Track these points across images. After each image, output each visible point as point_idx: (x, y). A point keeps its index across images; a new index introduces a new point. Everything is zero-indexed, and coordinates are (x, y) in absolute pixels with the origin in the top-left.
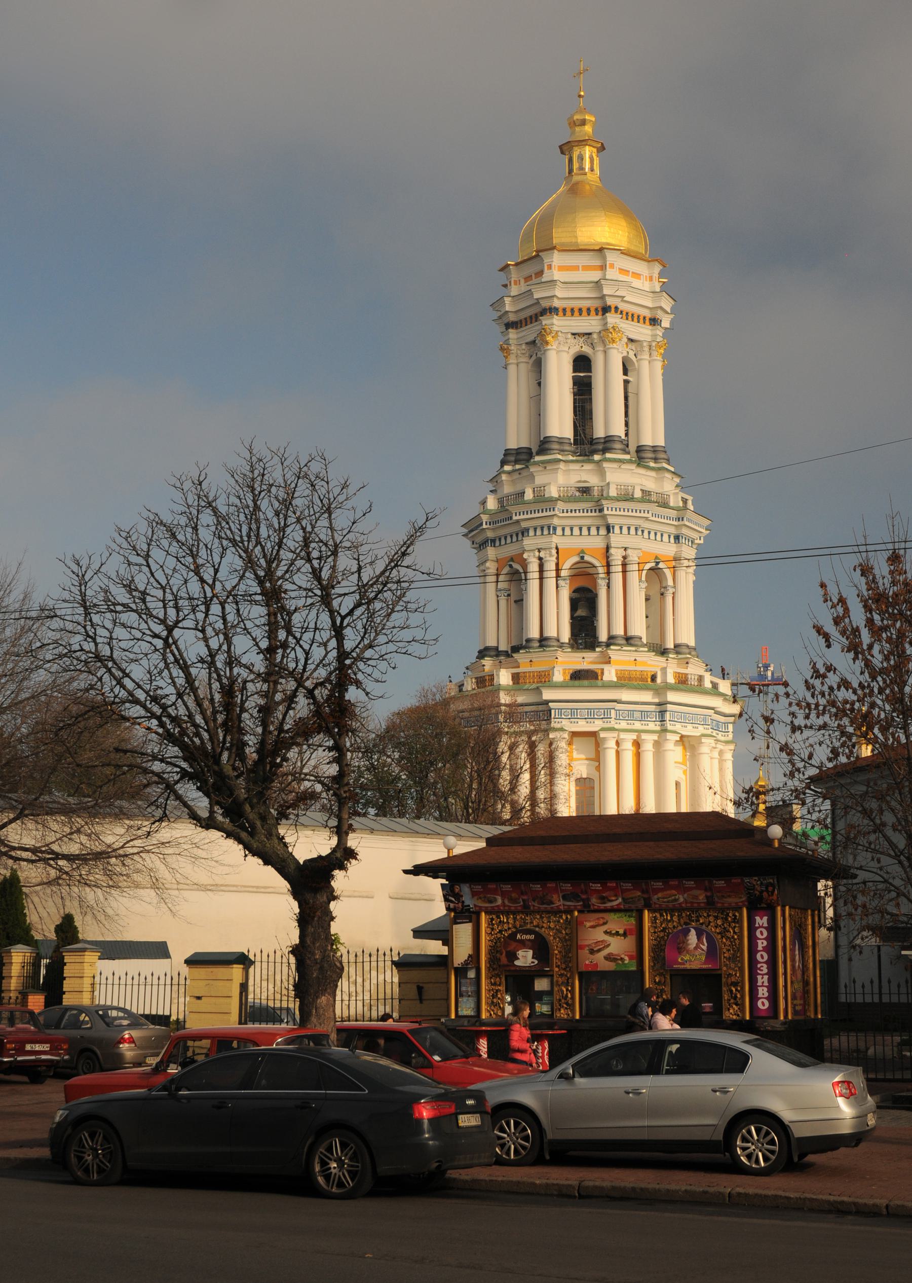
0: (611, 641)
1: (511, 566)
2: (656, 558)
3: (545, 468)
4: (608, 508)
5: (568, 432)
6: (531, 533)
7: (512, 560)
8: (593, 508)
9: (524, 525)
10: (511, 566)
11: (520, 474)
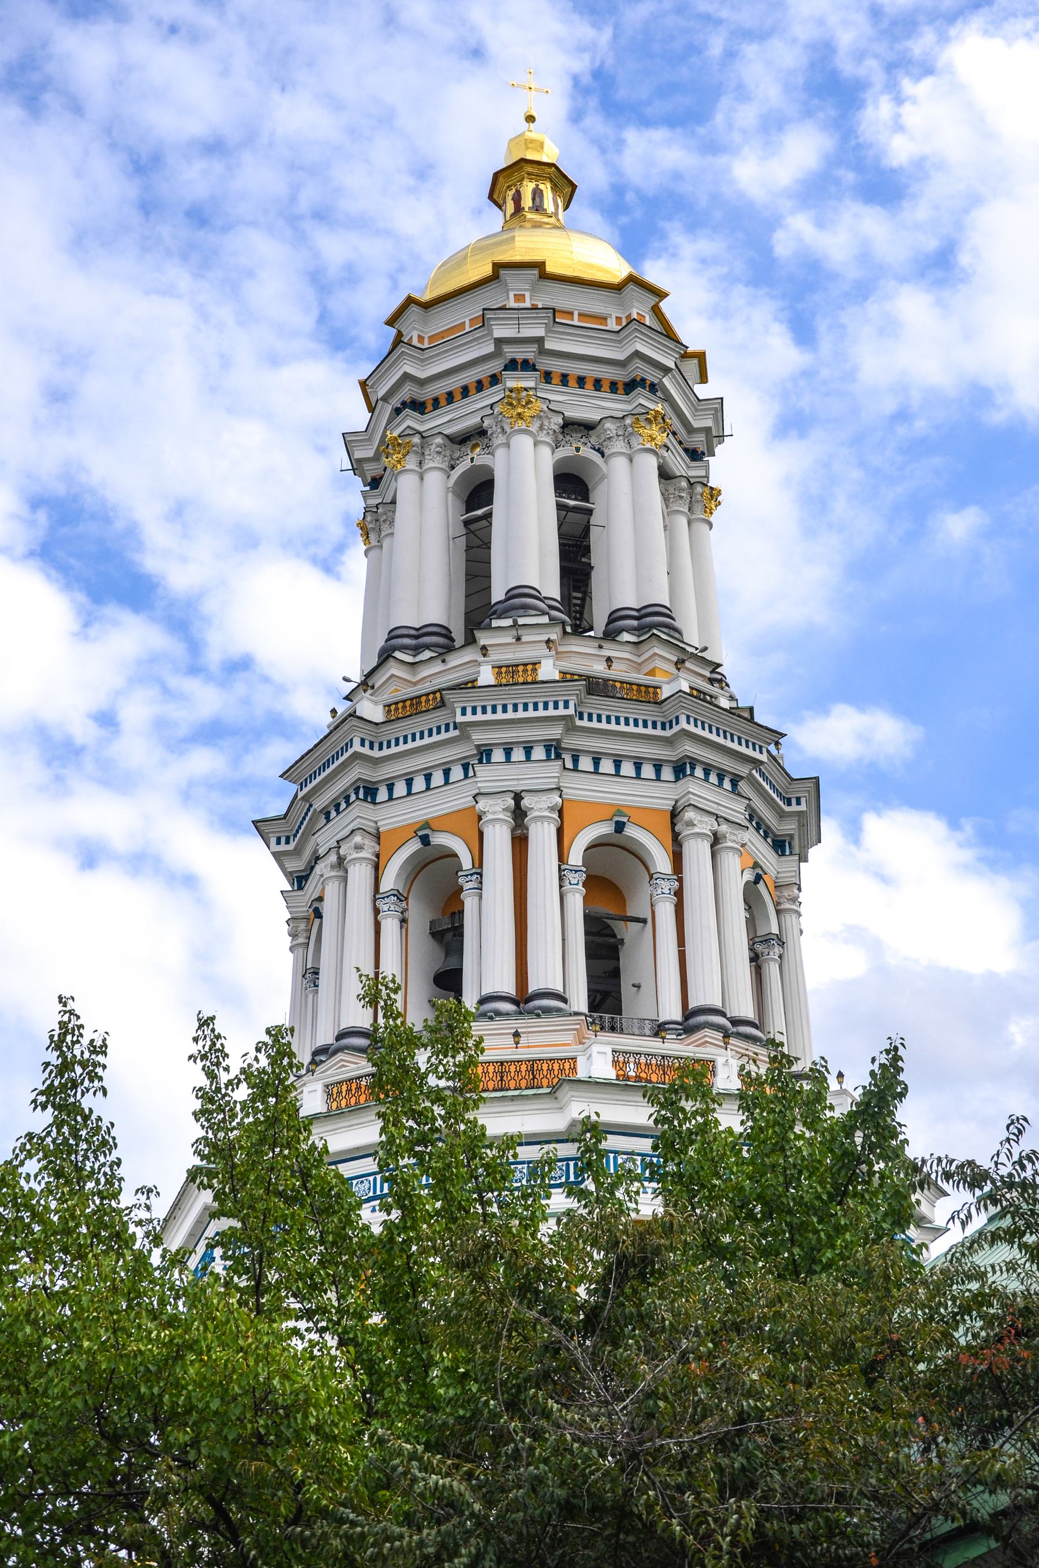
0: (693, 1021)
1: (425, 840)
2: (756, 865)
3: (518, 639)
4: (688, 717)
5: (552, 588)
6: (498, 755)
7: (426, 825)
8: (650, 720)
9: (479, 737)
10: (425, 840)
11: (443, 661)
